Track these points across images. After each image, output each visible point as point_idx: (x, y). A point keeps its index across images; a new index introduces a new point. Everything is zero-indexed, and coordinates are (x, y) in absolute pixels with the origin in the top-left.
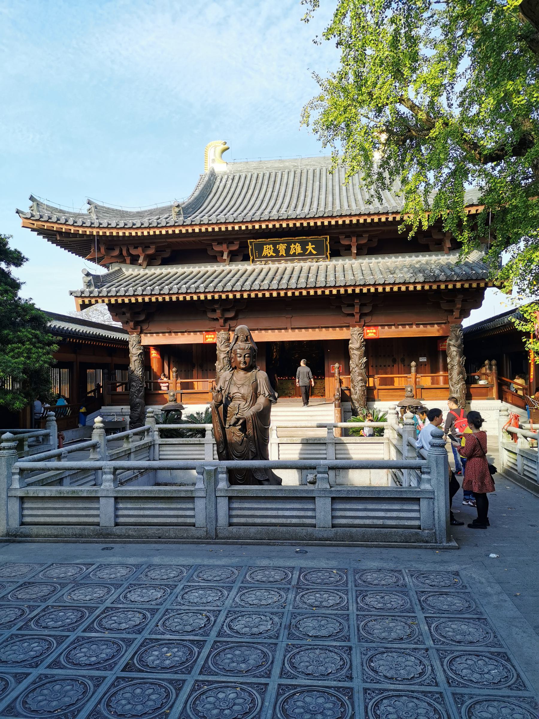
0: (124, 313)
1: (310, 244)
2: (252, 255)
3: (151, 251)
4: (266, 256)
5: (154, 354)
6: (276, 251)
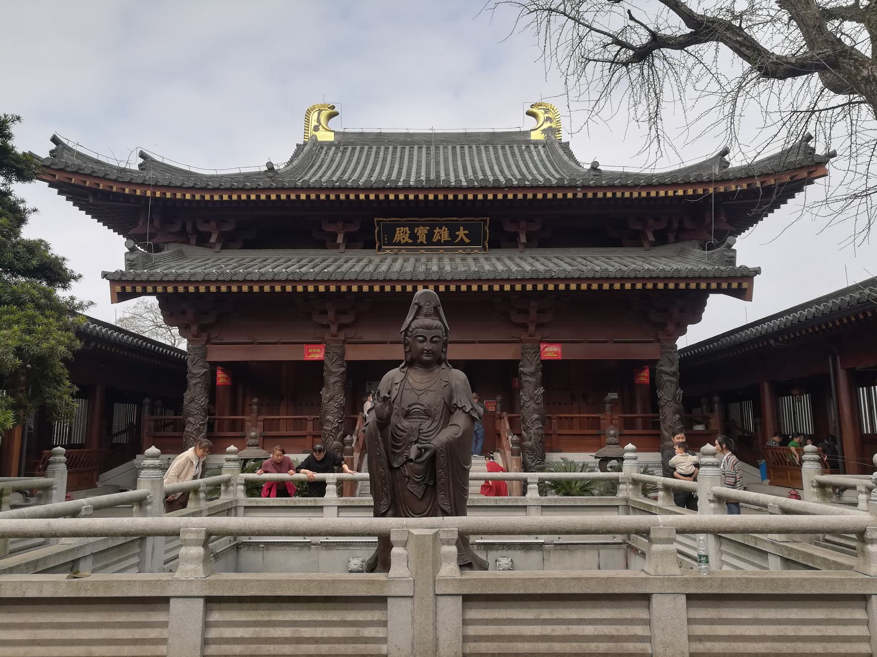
0: (184, 313)
1: (462, 228)
2: (379, 240)
3: (228, 228)
4: (399, 244)
5: (221, 378)
6: (414, 236)
